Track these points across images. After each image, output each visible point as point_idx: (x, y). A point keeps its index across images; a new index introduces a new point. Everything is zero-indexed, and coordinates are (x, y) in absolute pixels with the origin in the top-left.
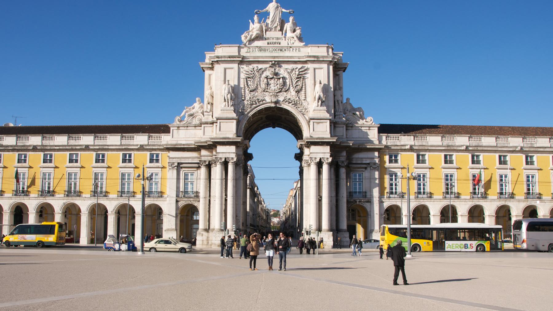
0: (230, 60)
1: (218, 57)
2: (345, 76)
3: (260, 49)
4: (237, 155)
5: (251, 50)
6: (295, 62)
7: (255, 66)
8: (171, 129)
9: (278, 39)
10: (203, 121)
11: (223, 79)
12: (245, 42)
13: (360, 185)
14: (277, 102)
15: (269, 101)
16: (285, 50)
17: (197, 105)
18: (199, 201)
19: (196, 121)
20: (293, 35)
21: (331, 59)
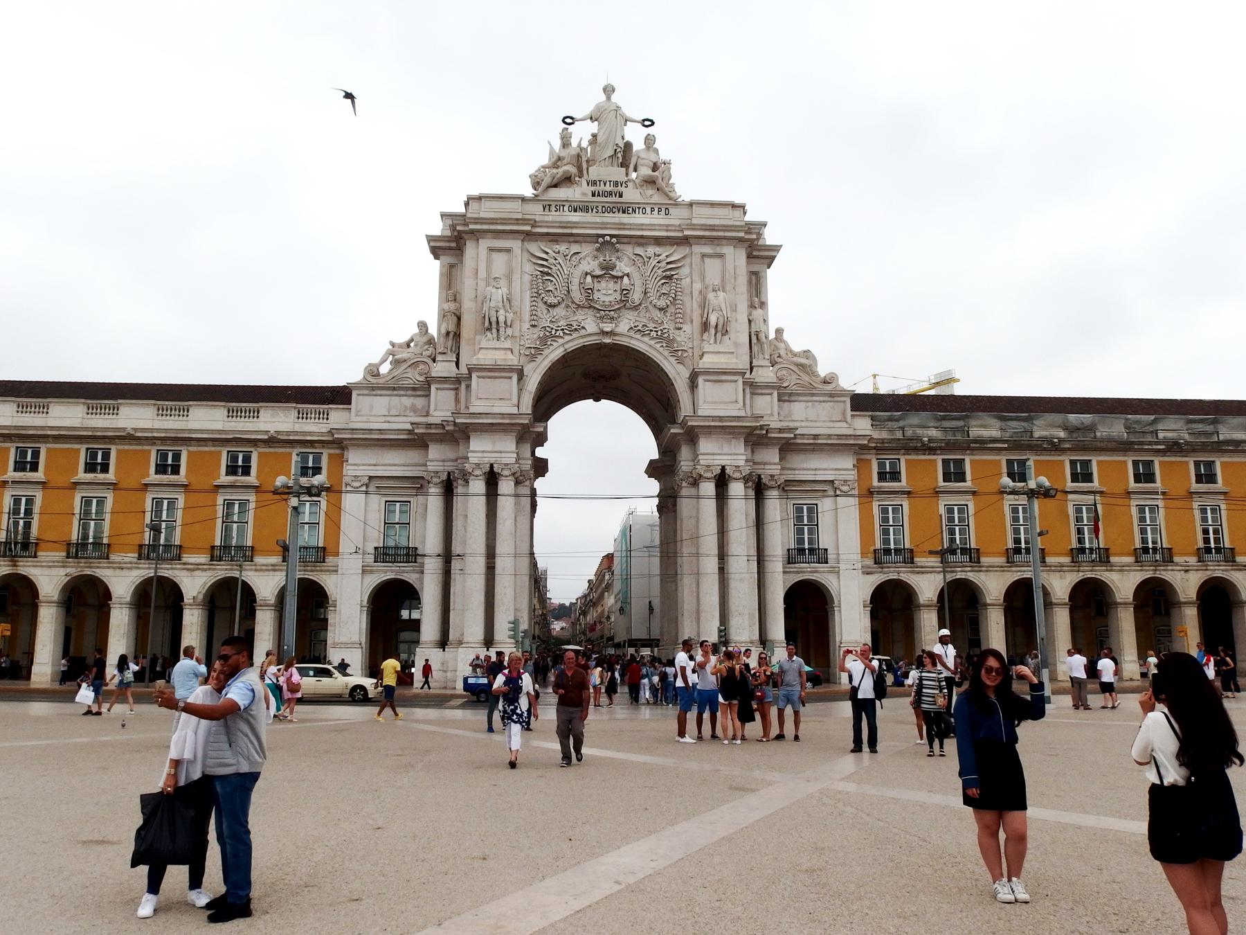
2: (774, 276)
6: (658, 241)
7: (562, 248)
9: (616, 184)
11: (482, 273)
13: (810, 532)
15: (596, 330)
16: (634, 211)
21: (742, 234)
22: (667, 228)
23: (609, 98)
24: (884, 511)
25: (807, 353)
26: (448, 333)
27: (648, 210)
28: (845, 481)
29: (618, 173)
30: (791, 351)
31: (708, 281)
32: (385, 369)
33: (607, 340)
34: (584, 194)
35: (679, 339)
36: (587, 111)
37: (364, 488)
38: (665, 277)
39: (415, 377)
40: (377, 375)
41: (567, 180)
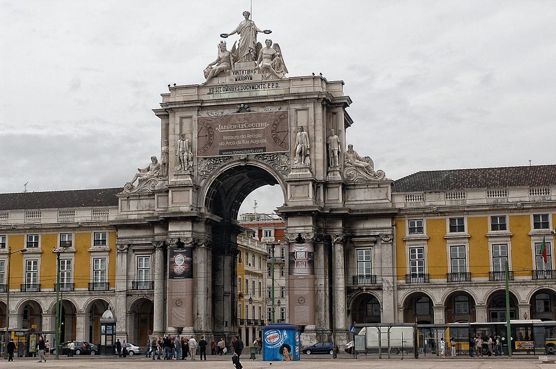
1: (171, 103)
3: (227, 88)
9: (249, 71)
11: (178, 131)
14: (246, 160)
22: (275, 96)
23: (247, 19)
24: (413, 251)
25: (368, 159)
28: (387, 236)
29: (250, 65)
30: (358, 158)
32: (136, 184)
34: (231, 80)
35: (283, 160)
36: (235, 29)
37: (126, 251)
39: (149, 188)
40: (132, 188)
41: (221, 73)
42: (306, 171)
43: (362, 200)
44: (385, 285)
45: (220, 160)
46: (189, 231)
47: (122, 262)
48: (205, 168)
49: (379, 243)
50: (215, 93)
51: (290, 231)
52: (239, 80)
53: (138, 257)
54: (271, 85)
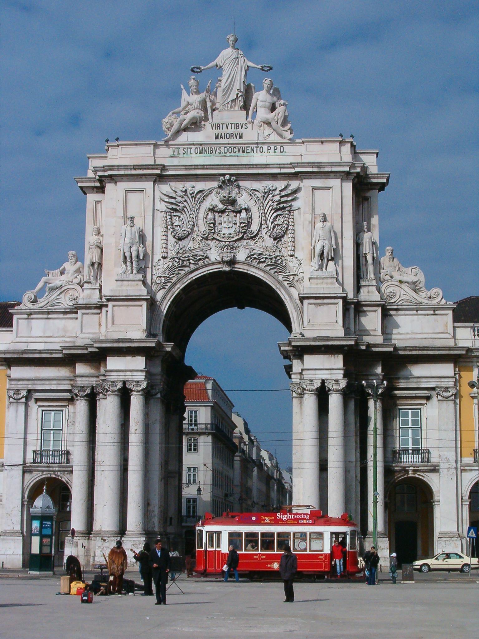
0: (136, 174)
1: (111, 168)
4: (149, 375)
5: (181, 151)
6: (274, 177)
7: (188, 185)
8: (15, 317)
9: (237, 126)
10: (80, 301)
12: (170, 134)
14: (232, 262)
15: (219, 259)
17: (70, 267)
18: (71, 472)
19: (66, 302)
20: (270, 116)
21: (347, 169)
22: (280, 166)
26: (93, 264)
27: (265, 148)
28: (447, 389)
31: (317, 212)
33: (226, 268)
35: (291, 265)
38: (280, 209)
42: (332, 283)
43: (408, 333)
44: (443, 467)
45: (189, 260)
46: (142, 371)
47: (16, 417)
48: (164, 272)
49: (435, 399)
50: (182, 155)
51: (307, 375)
52: (221, 137)
53: (43, 411)
54: (273, 148)
